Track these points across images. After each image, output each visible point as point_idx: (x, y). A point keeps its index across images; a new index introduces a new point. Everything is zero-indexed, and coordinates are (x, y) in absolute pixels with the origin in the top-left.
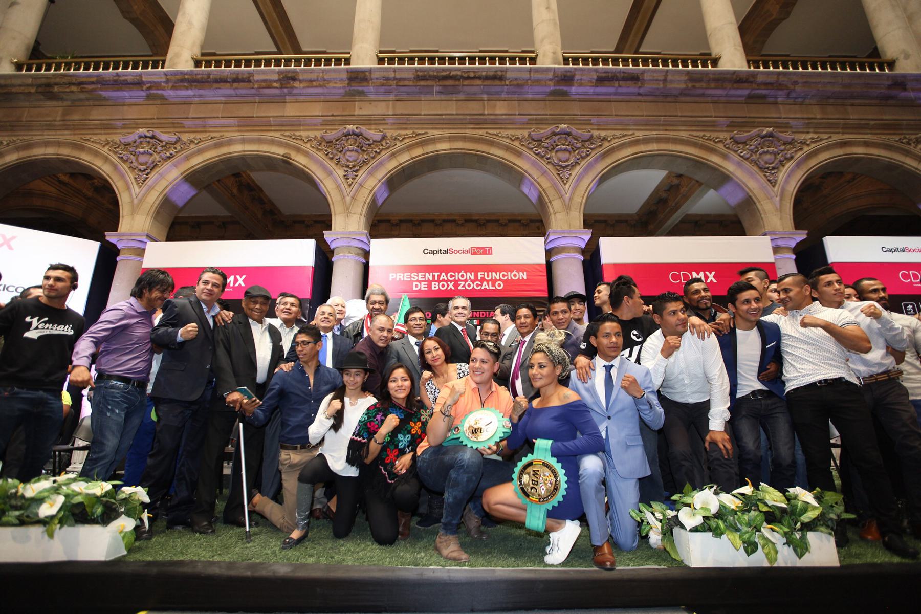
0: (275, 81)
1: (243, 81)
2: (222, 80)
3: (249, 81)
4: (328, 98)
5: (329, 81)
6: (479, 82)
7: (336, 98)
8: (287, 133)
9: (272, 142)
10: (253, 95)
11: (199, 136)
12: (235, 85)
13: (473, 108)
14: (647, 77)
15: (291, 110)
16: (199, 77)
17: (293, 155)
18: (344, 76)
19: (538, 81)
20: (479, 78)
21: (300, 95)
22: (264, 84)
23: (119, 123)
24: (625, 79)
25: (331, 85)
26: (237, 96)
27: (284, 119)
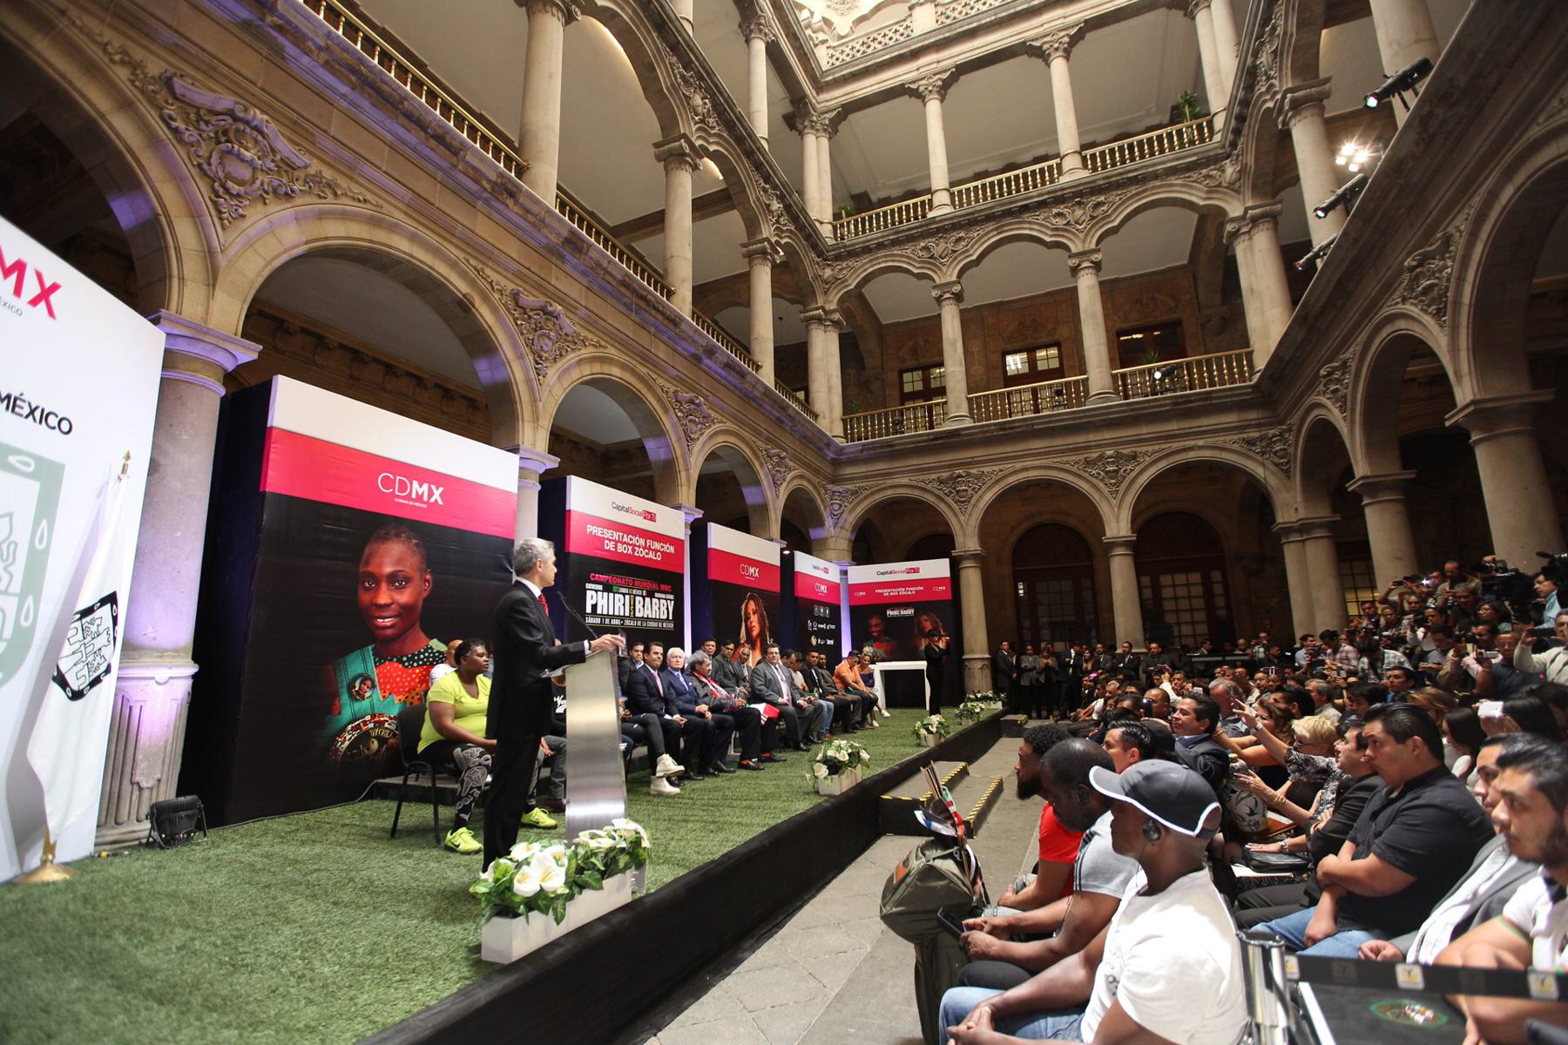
0: (489, 181)
1: (448, 147)
2: (418, 122)
3: (456, 154)
4: (525, 237)
5: (546, 225)
6: (660, 317)
7: (533, 243)
8: (472, 261)
9: (454, 265)
10: (440, 168)
11: (342, 182)
12: (433, 143)
13: (644, 339)
14: (748, 378)
15: (484, 229)
16: (385, 88)
17: (478, 301)
18: (565, 233)
19: (695, 342)
20: (663, 314)
21: (497, 211)
22: (471, 172)
23: (167, 35)
24: (634, 291)
25: (546, 231)
26: (414, 150)
27: (470, 235)
